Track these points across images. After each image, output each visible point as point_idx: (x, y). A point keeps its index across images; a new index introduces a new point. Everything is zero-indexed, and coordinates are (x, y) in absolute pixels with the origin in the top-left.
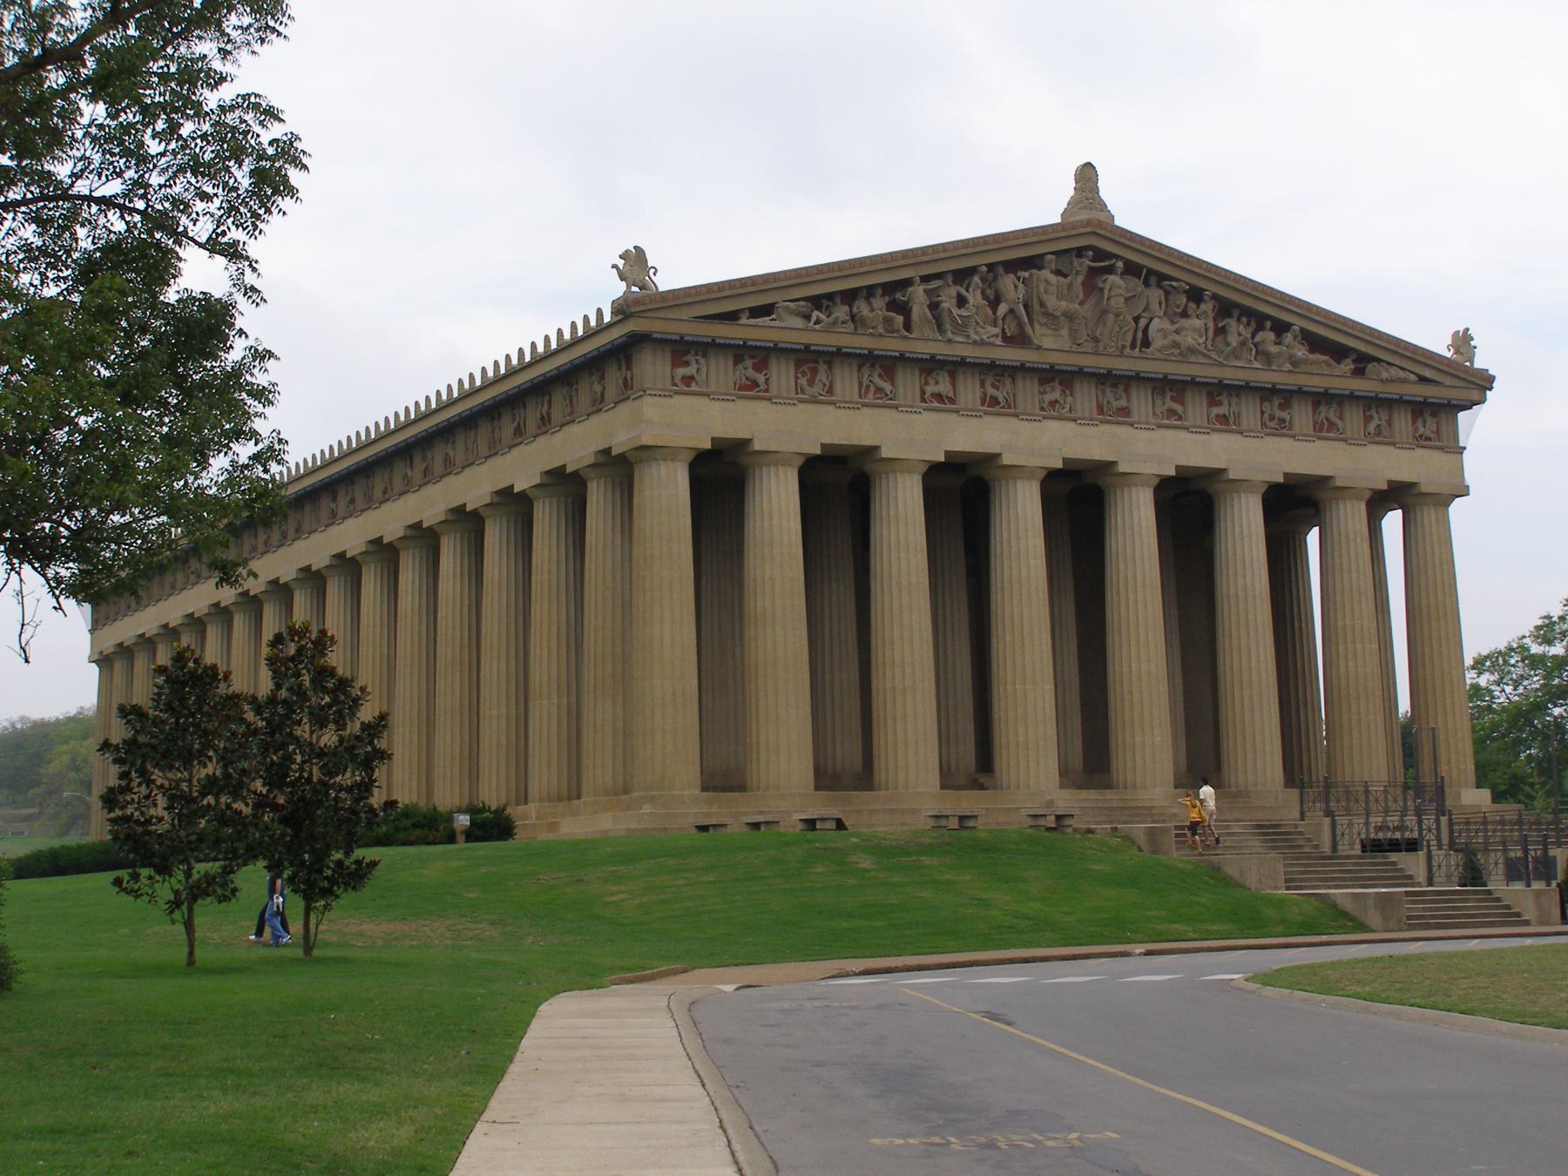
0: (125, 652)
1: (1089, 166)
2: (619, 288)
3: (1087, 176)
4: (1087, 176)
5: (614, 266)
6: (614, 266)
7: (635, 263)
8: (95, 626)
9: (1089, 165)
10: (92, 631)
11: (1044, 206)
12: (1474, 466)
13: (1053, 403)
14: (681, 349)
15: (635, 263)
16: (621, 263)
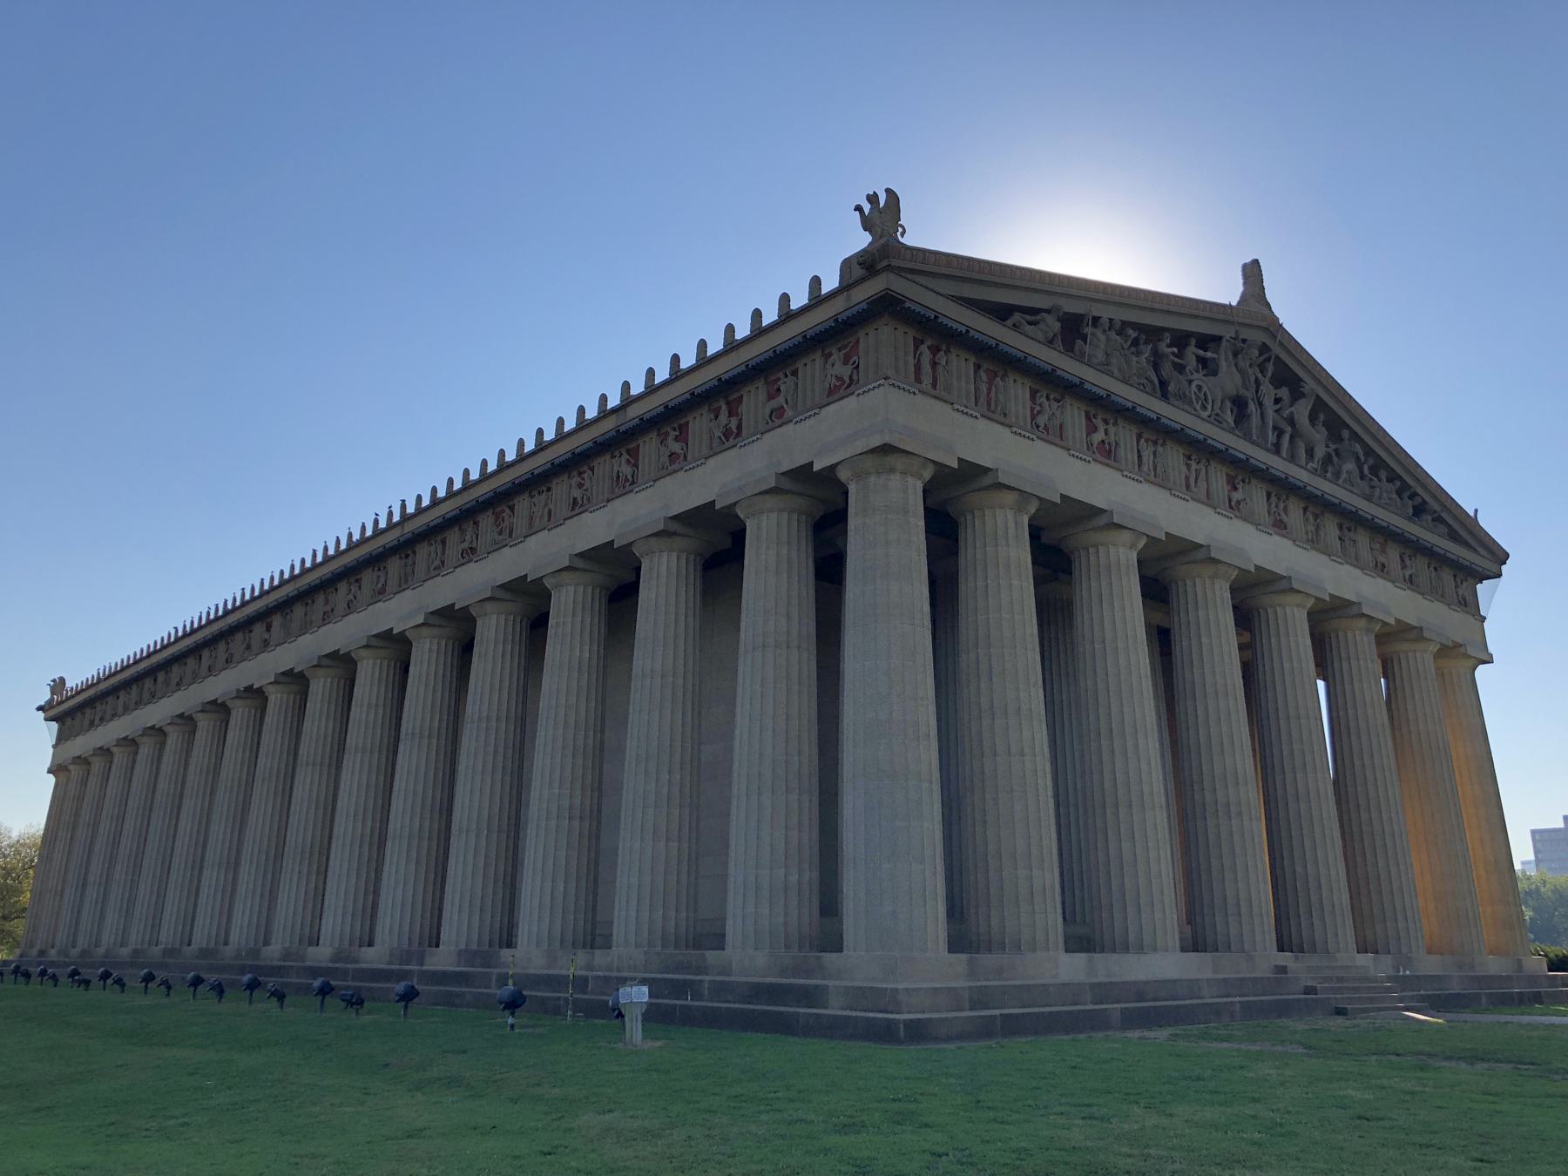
0: (81, 760)
1: (1256, 262)
2: (861, 240)
3: (1253, 273)
4: (1253, 273)
5: (859, 208)
6: (859, 208)
7: (882, 215)
8: (61, 739)
9: (1256, 262)
10: (54, 747)
11: (1229, 292)
12: (1495, 633)
13: (1238, 502)
14: (935, 334)
15: (882, 215)
16: (867, 208)
